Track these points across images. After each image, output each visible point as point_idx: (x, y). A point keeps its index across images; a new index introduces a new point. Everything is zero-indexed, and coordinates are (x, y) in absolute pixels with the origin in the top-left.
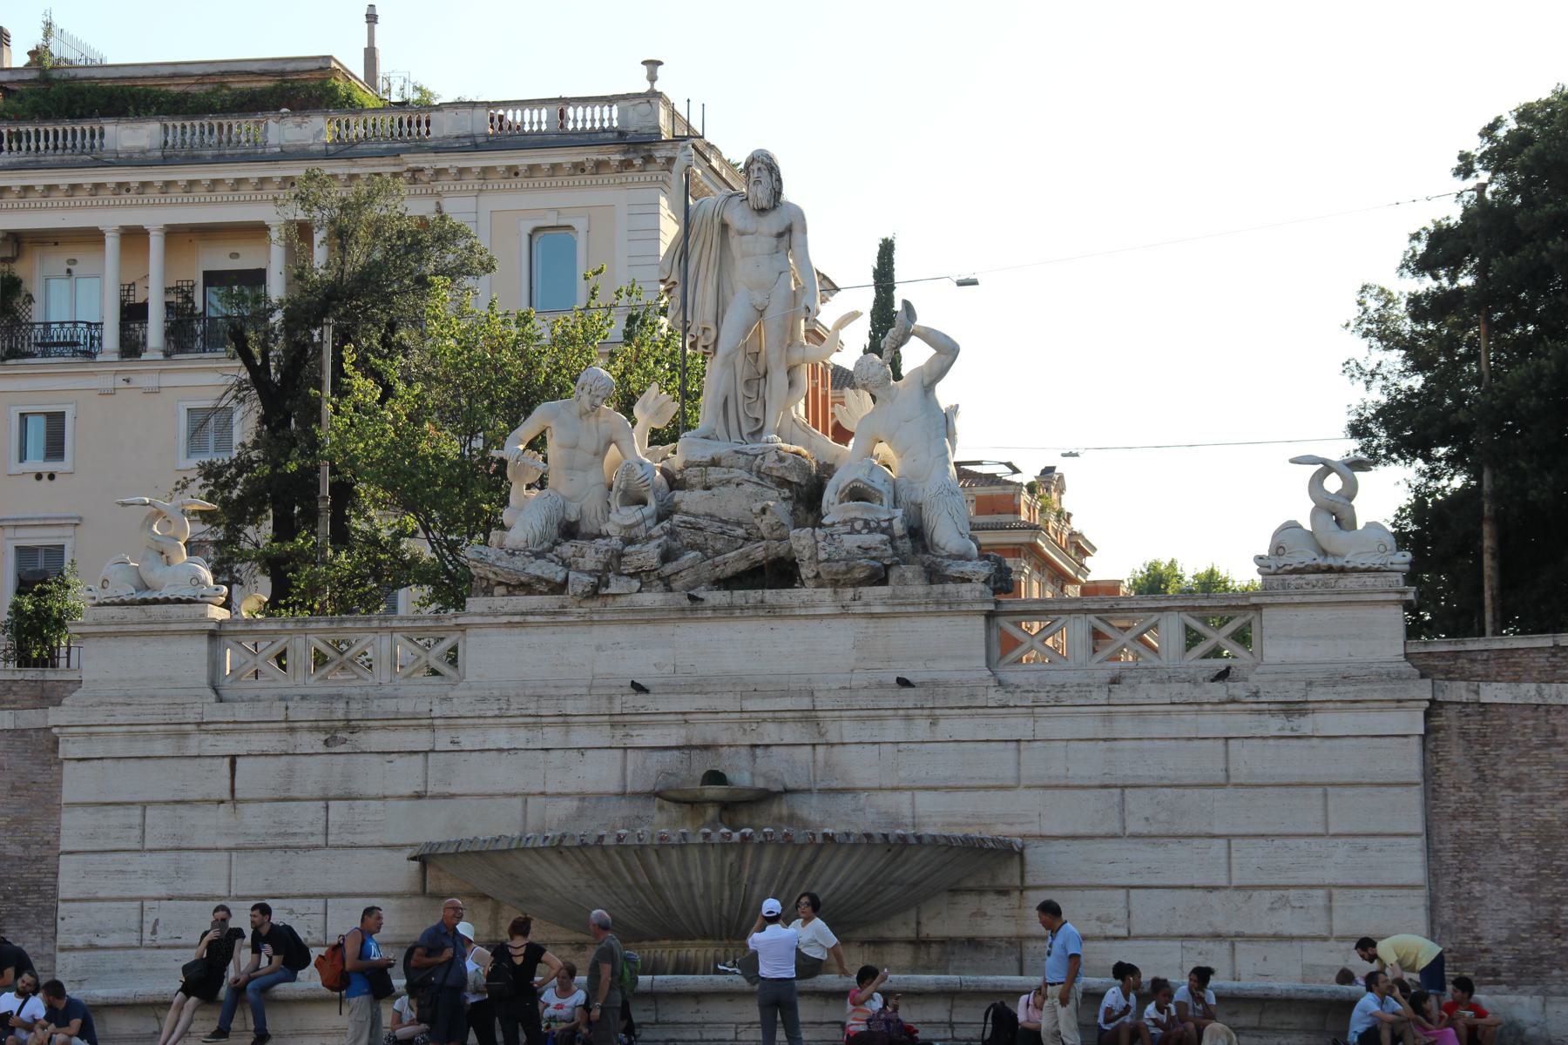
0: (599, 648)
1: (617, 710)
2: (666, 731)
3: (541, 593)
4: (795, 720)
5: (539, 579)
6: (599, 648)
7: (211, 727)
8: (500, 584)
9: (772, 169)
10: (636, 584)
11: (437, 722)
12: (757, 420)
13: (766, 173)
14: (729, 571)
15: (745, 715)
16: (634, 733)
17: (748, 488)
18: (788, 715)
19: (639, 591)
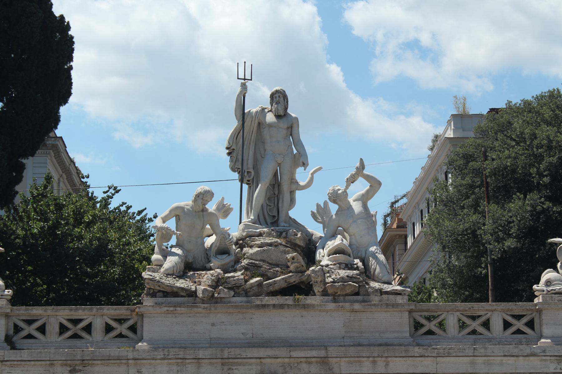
0: (213, 325)
1: (226, 355)
2: (250, 367)
3: (182, 296)
4: (317, 362)
5: (182, 289)
6: (213, 325)
7: (8, 363)
8: (160, 291)
9: (285, 97)
10: (232, 293)
11: (130, 362)
12: (274, 217)
13: (282, 99)
14: (277, 287)
15: (292, 360)
16: (234, 368)
17: (282, 248)
18: (313, 360)
19: (234, 296)
